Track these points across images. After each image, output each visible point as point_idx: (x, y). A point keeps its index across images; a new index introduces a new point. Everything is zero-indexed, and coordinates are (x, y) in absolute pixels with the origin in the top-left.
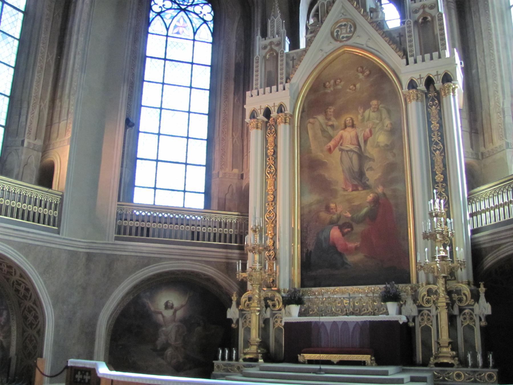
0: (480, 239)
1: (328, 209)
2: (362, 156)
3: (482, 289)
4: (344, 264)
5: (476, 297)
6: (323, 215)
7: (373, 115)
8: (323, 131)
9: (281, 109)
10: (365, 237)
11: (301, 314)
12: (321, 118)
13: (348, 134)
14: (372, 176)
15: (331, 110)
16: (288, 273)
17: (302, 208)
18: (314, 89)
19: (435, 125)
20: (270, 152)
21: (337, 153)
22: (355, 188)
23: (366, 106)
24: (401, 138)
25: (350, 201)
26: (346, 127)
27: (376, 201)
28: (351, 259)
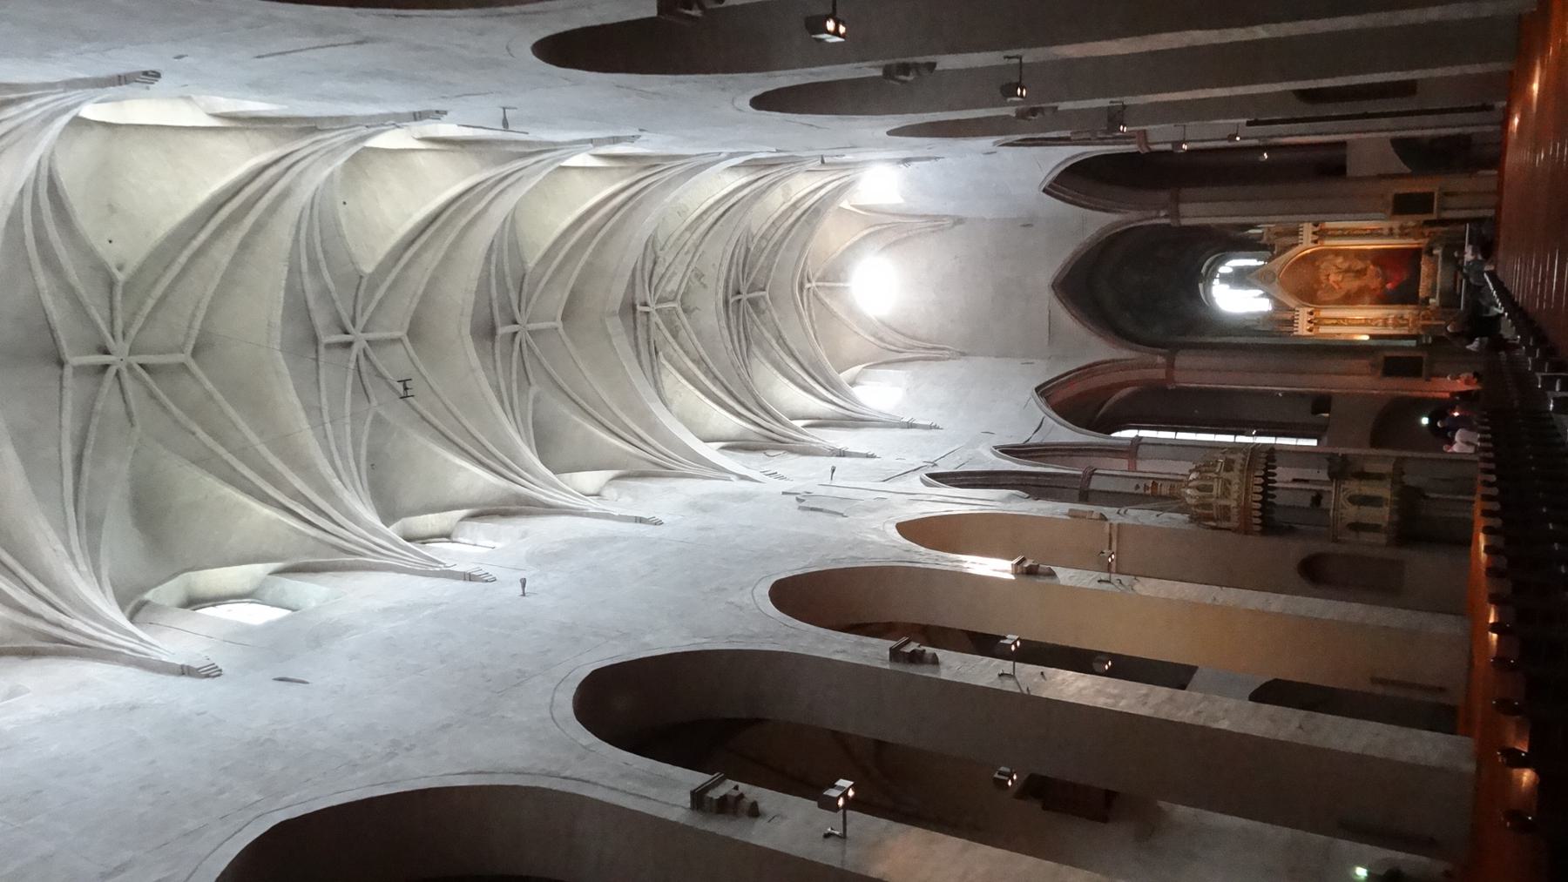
0: (1385, 225)
2: (1348, 271)
13: (1332, 278)
14: (1360, 265)
16: (1408, 312)
25: (1372, 280)
27: (1375, 263)
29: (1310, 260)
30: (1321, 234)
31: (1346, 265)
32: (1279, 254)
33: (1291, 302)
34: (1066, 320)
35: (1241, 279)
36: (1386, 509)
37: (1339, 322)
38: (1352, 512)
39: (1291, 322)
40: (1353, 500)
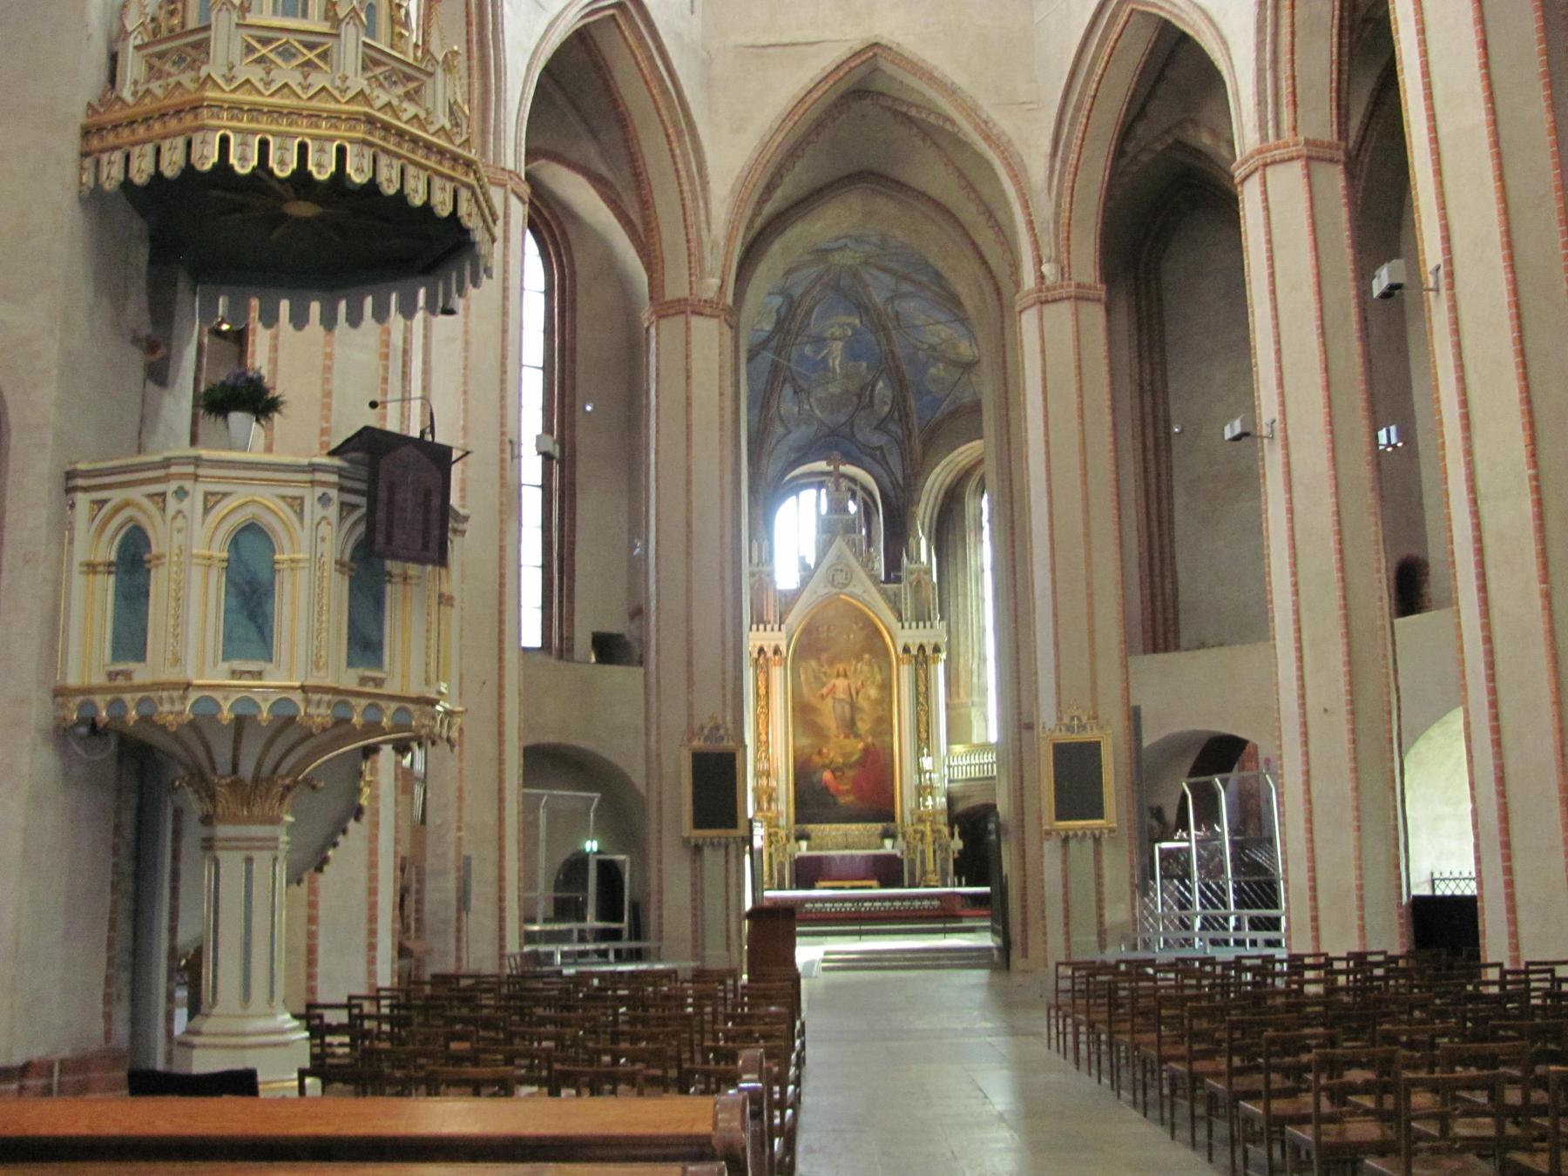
1: (820, 752)
2: (854, 707)
3: (956, 830)
4: (835, 804)
5: (952, 836)
6: (816, 758)
7: (865, 668)
8: (816, 677)
9: (776, 651)
10: (855, 781)
11: (809, 848)
12: (813, 663)
13: (841, 683)
14: (863, 727)
15: (824, 657)
17: (795, 750)
18: (803, 633)
19: (922, 688)
20: (762, 691)
21: (829, 700)
22: (847, 736)
23: (859, 658)
24: (891, 695)
25: (841, 748)
26: (838, 675)
27: (866, 750)
28: (842, 800)
29: (873, 642)
30: (921, 658)
31: (862, 702)
32: (883, 592)
33: (795, 619)
34: (787, 86)
35: (833, 528)
36: (218, 675)
37: (764, 699)
38: (192, 547)
39: (759, 619)
40: (251, 538)
